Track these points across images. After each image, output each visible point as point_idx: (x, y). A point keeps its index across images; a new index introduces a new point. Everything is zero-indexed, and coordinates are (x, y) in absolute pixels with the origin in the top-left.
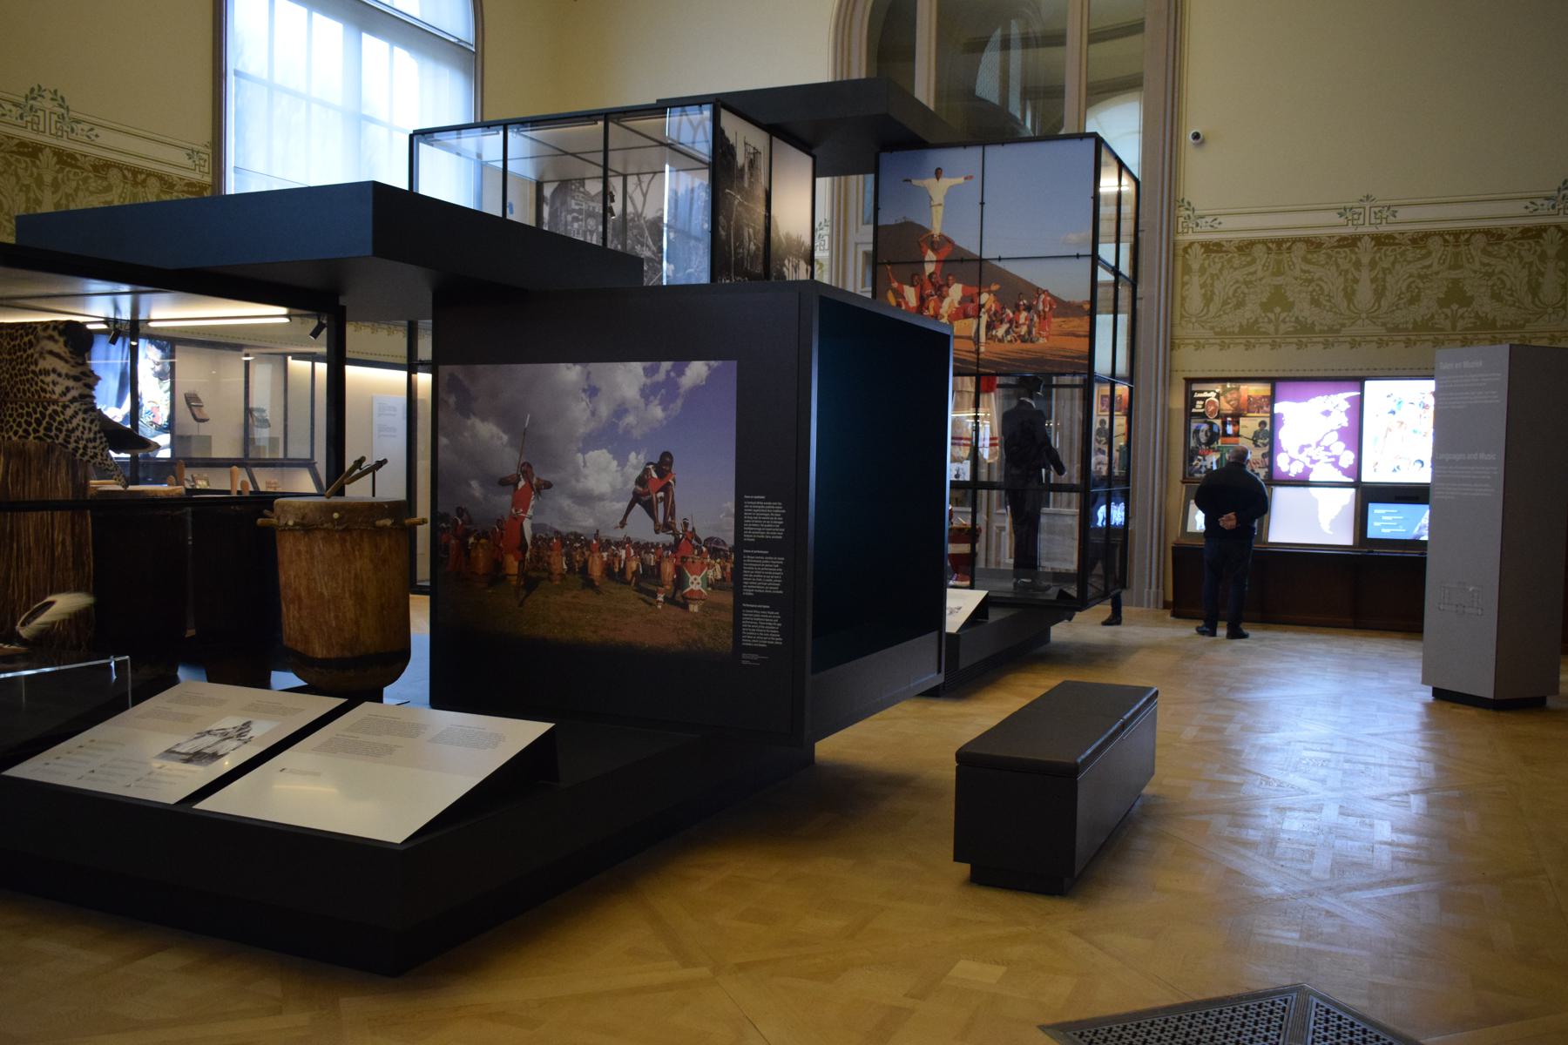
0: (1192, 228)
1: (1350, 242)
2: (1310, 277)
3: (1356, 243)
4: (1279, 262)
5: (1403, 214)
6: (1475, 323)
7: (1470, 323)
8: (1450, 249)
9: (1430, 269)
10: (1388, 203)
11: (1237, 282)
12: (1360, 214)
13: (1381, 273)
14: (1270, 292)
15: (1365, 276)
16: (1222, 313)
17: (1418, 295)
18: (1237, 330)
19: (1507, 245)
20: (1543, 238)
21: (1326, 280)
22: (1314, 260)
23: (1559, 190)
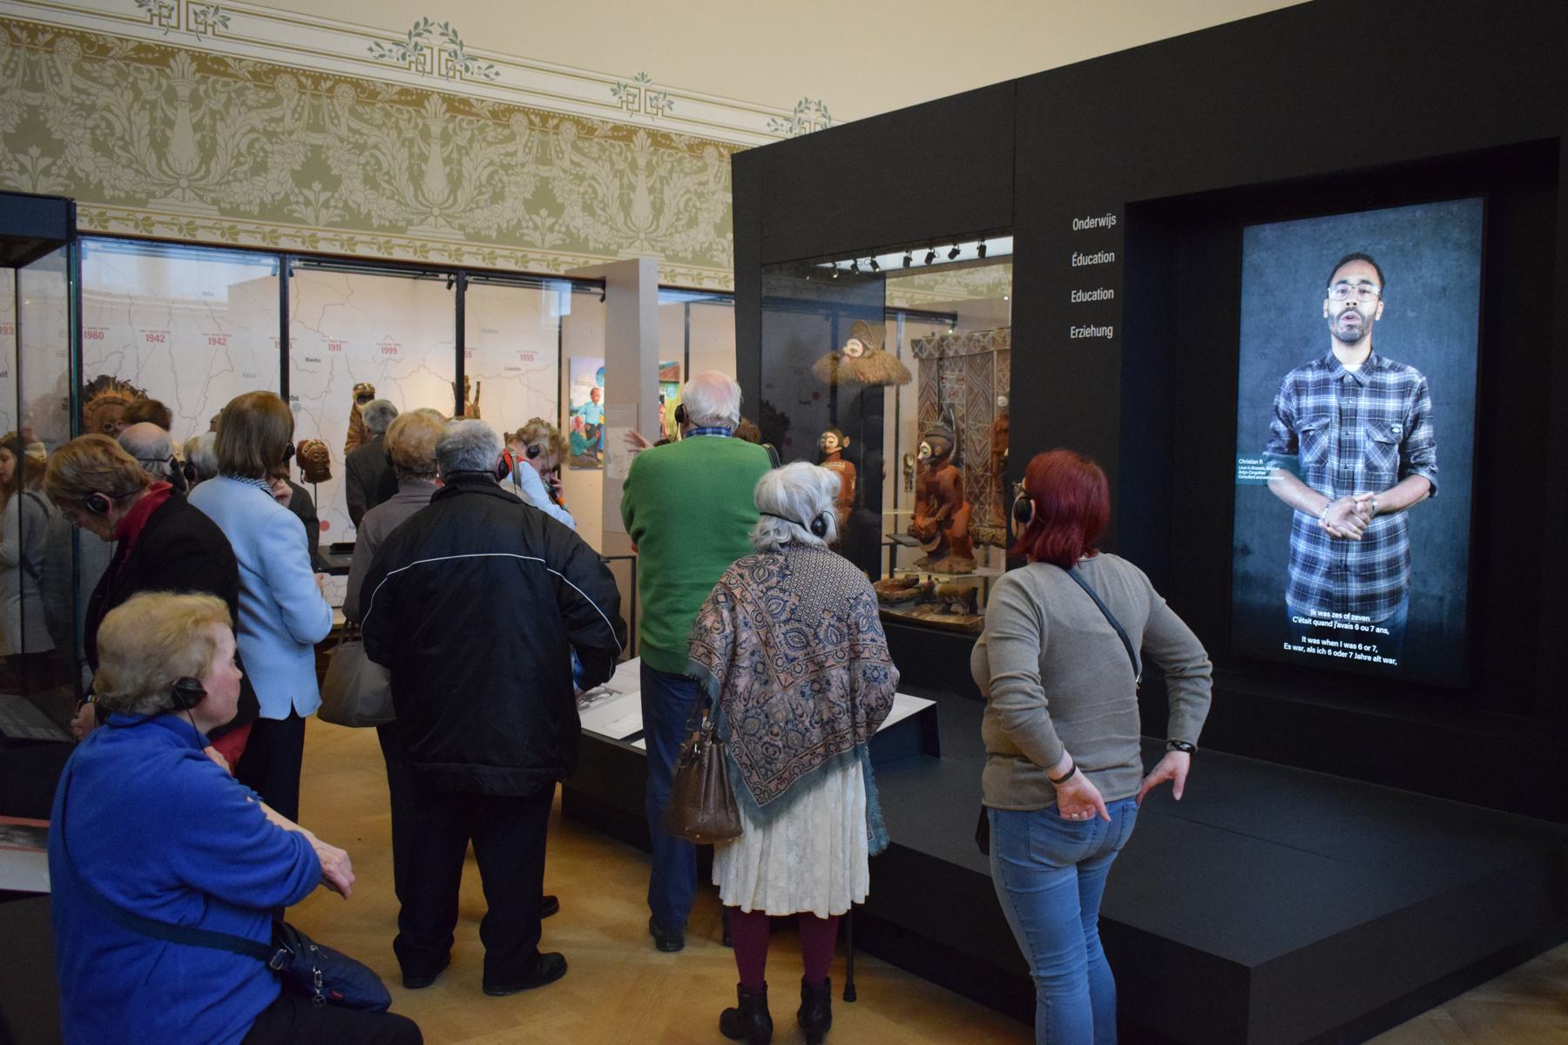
0: (461, 72)
1: (625, 134)
2: (88, 103)
3: (423, 102)
4: (544, 145)
5: (681, 108)
6: (564, 240)
7: (339, 216)
8: (536, 134)
9: (281, 125)
10: (664, 89)
11: (253, 130)
12: (172, 9)
13: (455, 151)
14: (20, 116)
15: (642, 182)
16: (474, 206)
17: (696, 218)
18: (690, 256)
19: (597, 143)
20: (424, 107)
21: (116, 111)
22: (95, 74)
23: (795, 111)
